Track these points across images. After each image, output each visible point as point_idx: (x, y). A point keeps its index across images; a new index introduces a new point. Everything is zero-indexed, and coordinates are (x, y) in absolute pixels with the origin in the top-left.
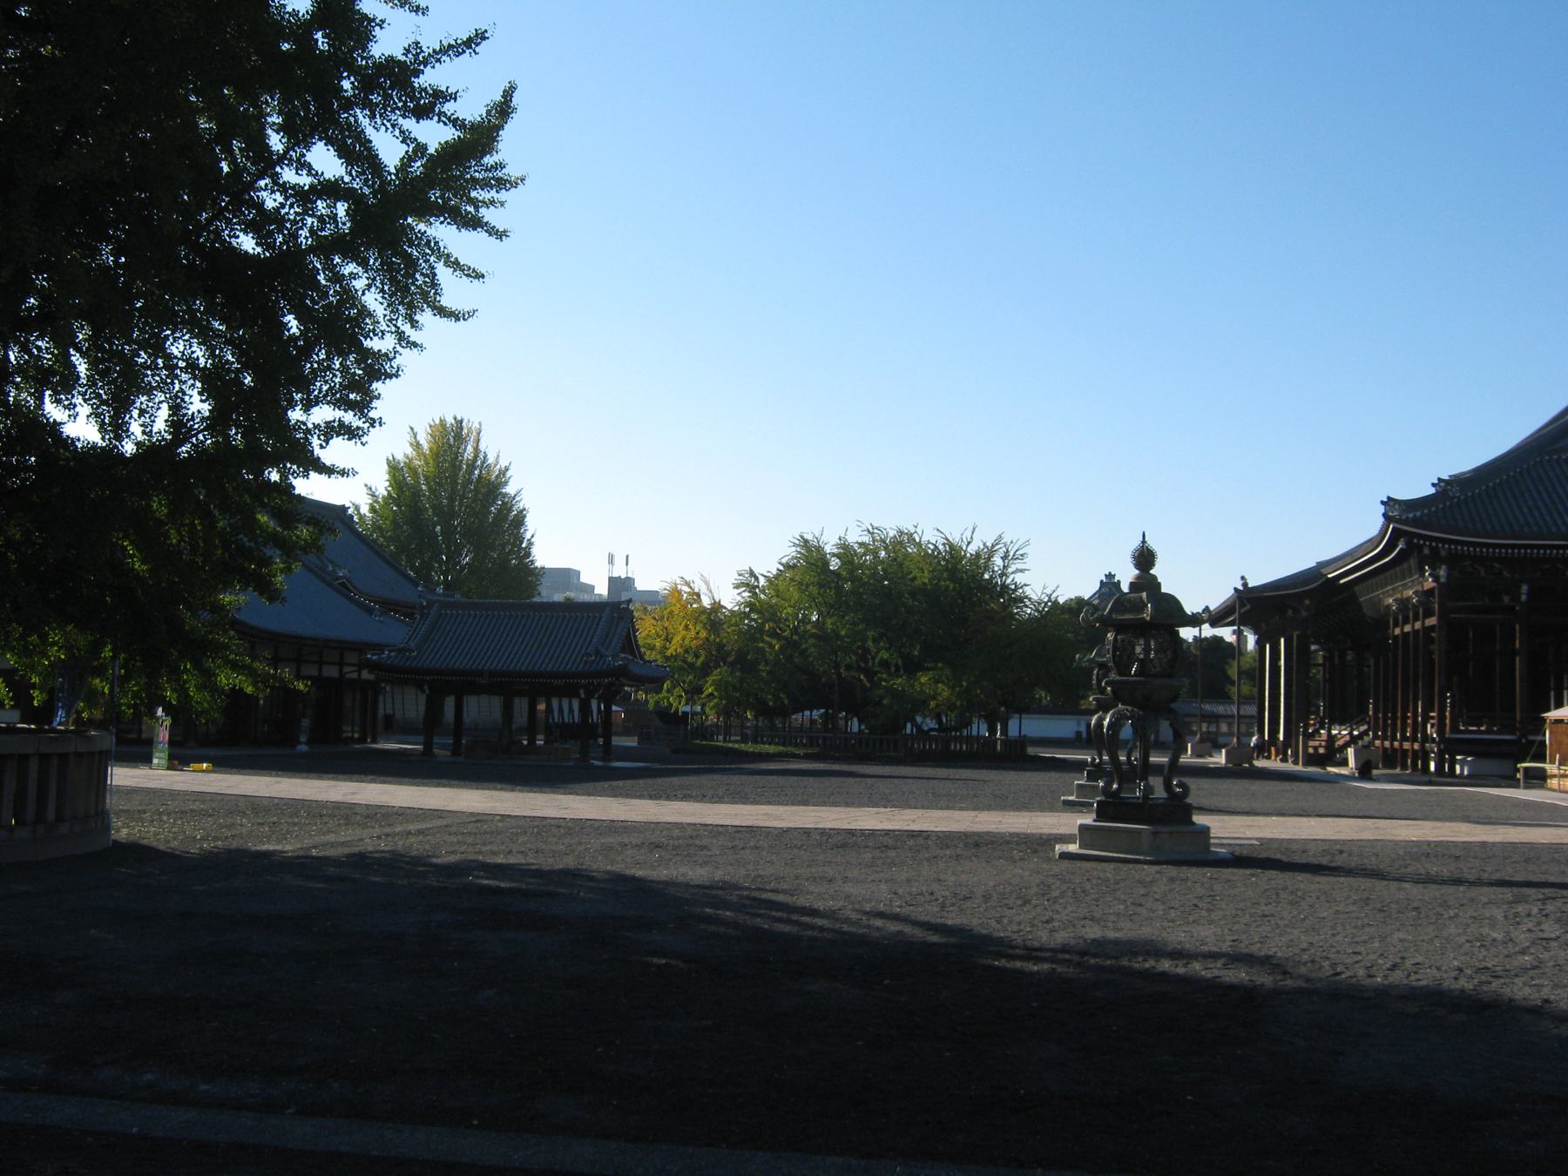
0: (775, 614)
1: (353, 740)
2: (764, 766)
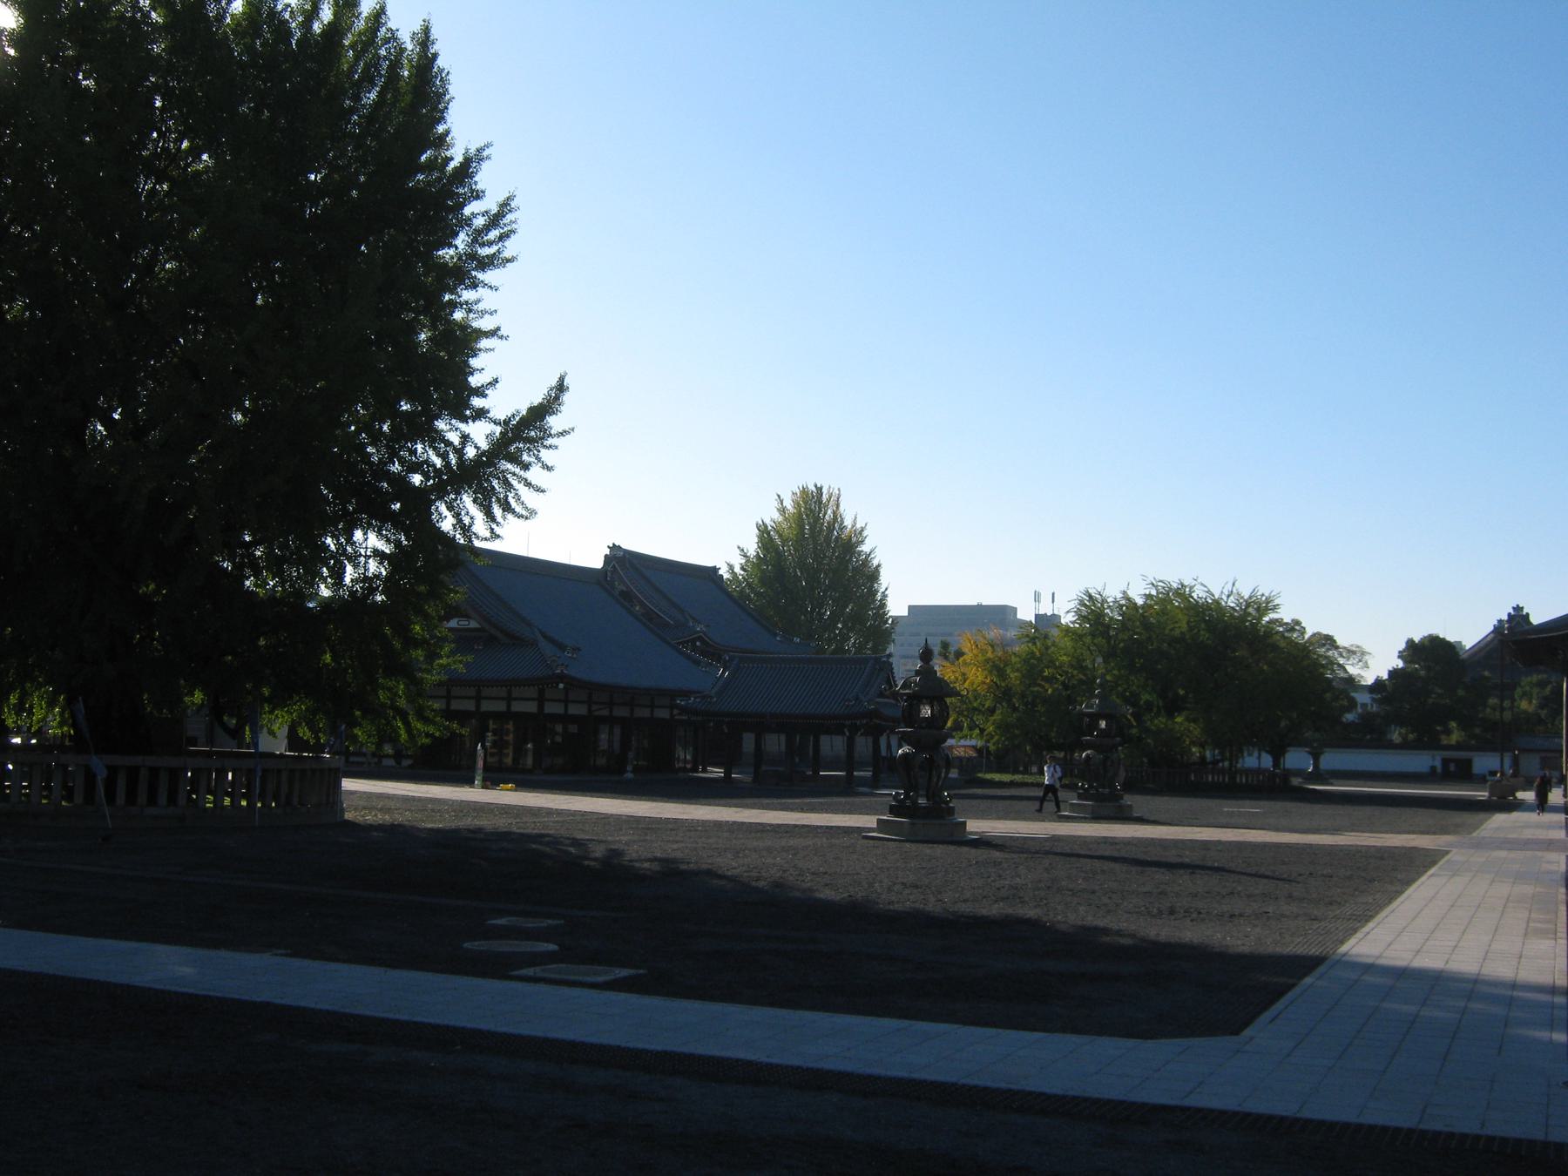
0: (1052, 662)
1: (684, 770)
2: (999, 792)
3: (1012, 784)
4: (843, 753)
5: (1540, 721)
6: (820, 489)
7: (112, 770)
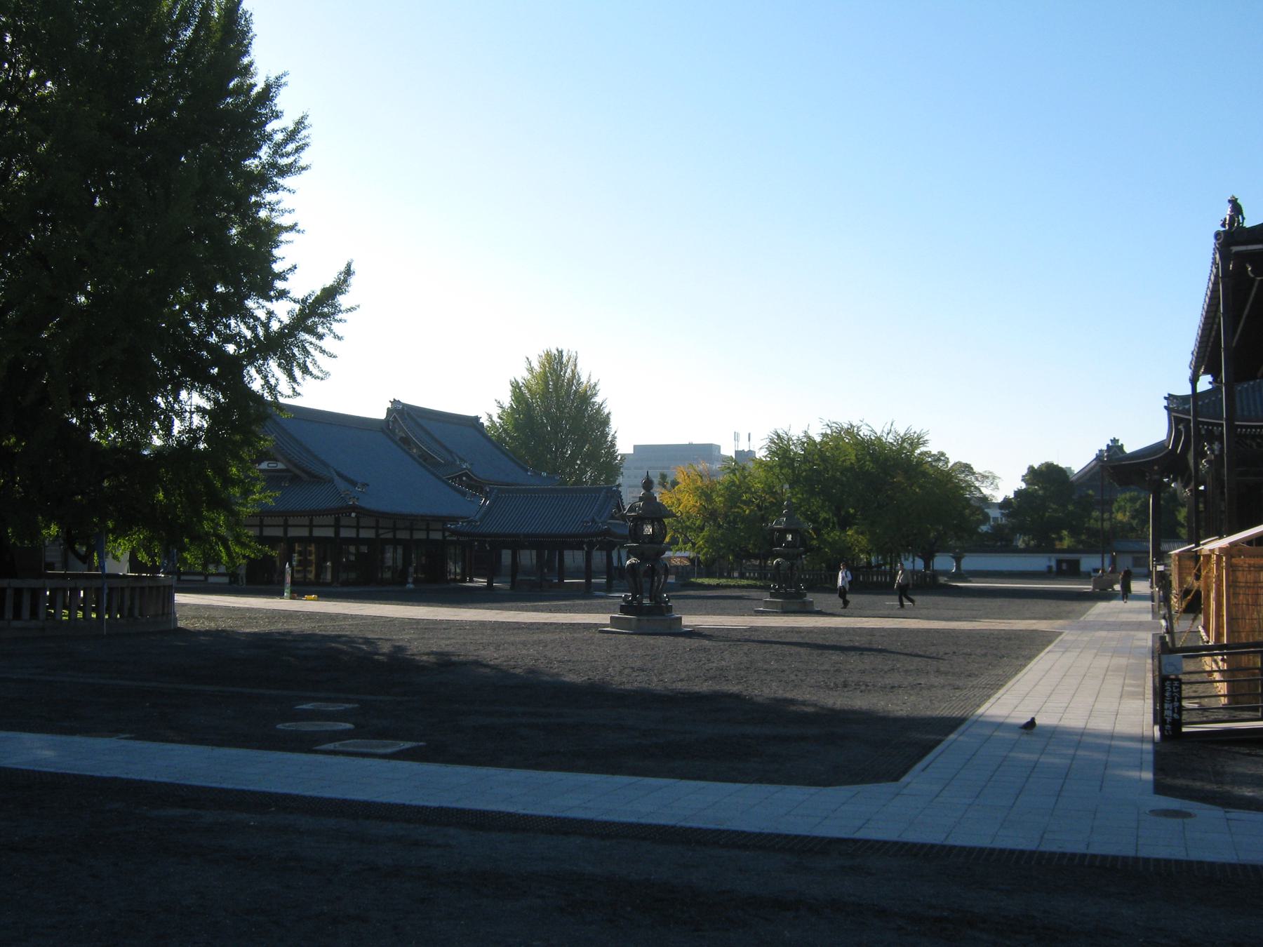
0: (749, 488)
1: (455, 580)
3: (718, 587)
4: (583, 565)
5: (1132, 529)
6: (561, 353)
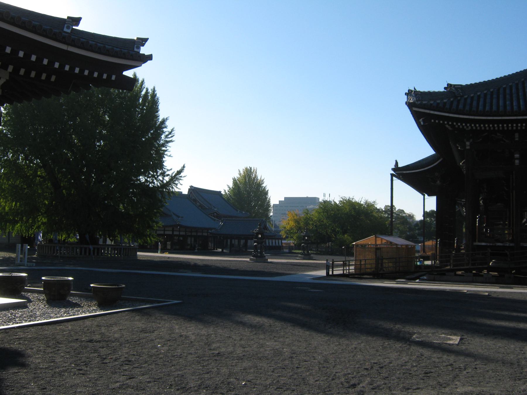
1: (211, 249)
6: (251, 168)
7: (94, 248)
